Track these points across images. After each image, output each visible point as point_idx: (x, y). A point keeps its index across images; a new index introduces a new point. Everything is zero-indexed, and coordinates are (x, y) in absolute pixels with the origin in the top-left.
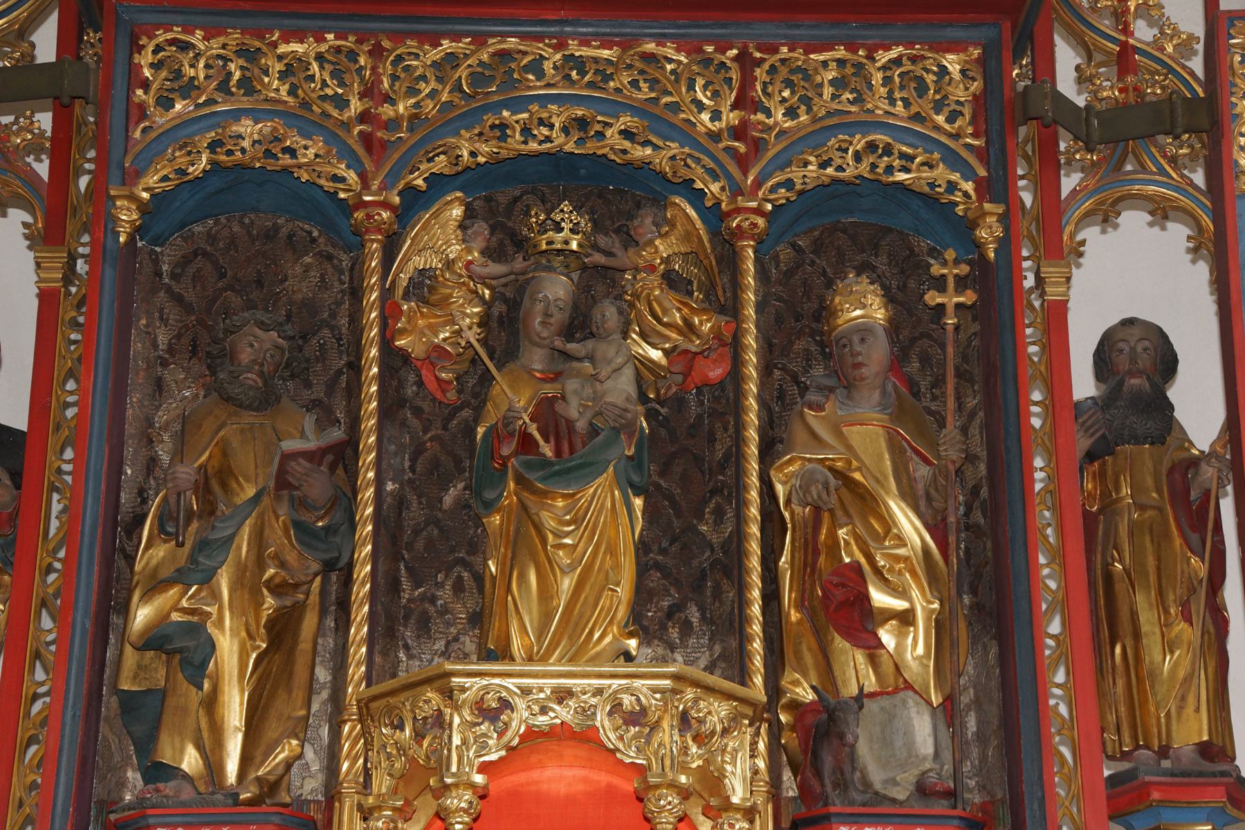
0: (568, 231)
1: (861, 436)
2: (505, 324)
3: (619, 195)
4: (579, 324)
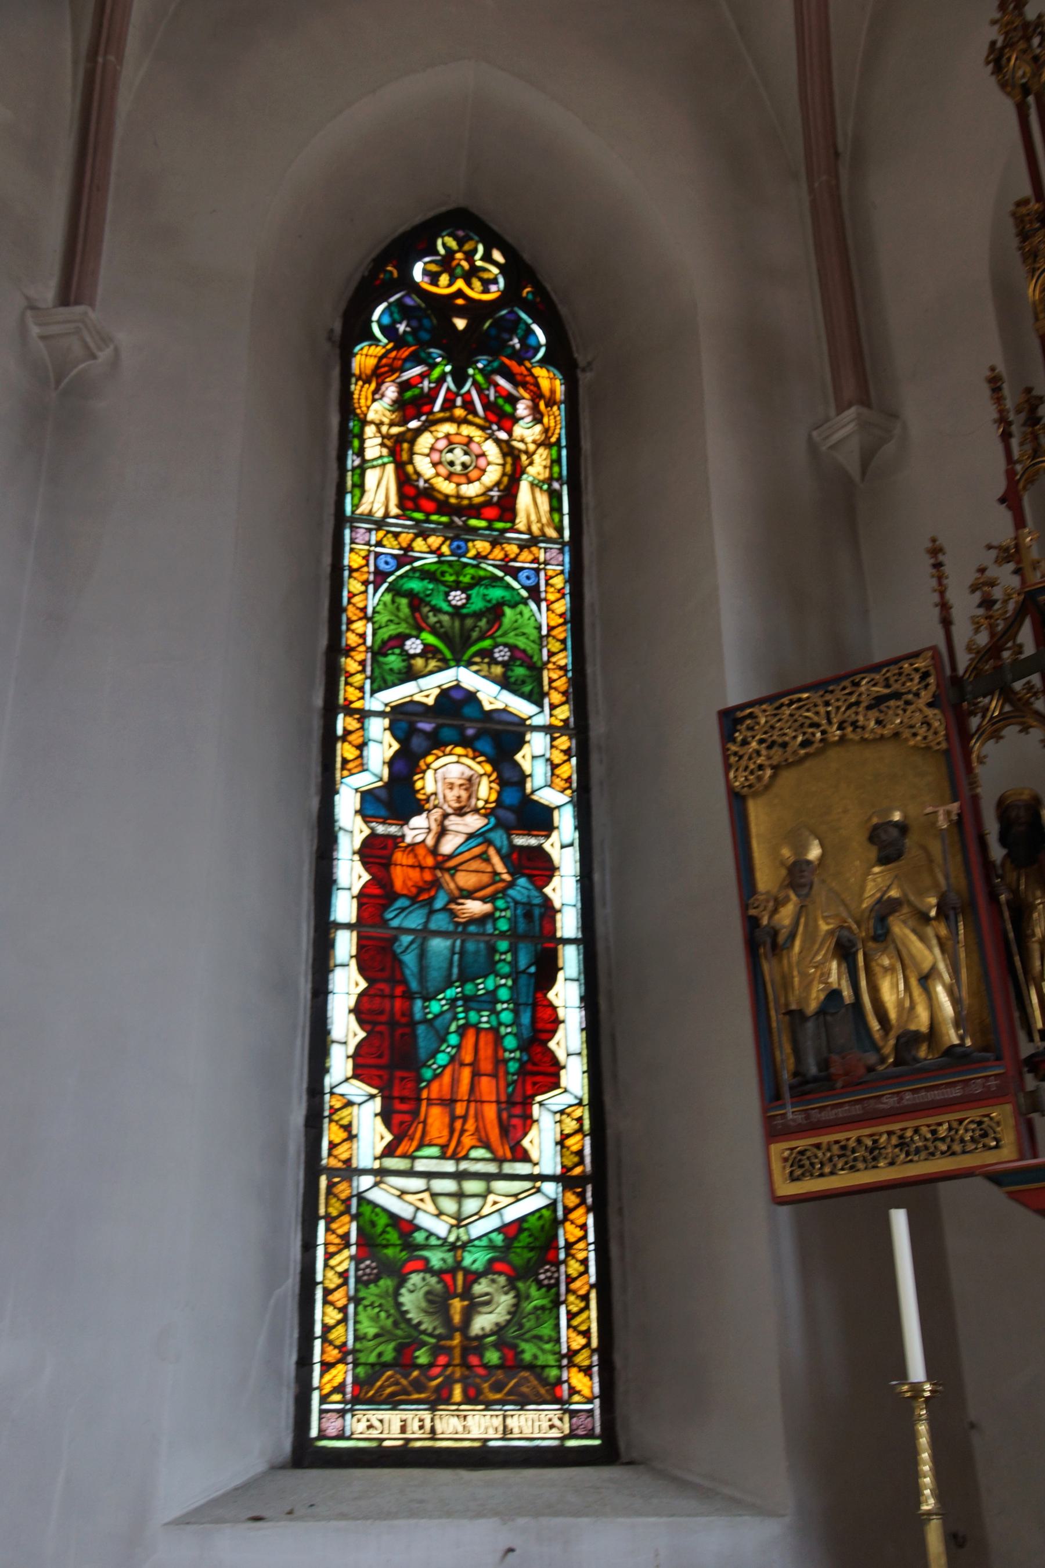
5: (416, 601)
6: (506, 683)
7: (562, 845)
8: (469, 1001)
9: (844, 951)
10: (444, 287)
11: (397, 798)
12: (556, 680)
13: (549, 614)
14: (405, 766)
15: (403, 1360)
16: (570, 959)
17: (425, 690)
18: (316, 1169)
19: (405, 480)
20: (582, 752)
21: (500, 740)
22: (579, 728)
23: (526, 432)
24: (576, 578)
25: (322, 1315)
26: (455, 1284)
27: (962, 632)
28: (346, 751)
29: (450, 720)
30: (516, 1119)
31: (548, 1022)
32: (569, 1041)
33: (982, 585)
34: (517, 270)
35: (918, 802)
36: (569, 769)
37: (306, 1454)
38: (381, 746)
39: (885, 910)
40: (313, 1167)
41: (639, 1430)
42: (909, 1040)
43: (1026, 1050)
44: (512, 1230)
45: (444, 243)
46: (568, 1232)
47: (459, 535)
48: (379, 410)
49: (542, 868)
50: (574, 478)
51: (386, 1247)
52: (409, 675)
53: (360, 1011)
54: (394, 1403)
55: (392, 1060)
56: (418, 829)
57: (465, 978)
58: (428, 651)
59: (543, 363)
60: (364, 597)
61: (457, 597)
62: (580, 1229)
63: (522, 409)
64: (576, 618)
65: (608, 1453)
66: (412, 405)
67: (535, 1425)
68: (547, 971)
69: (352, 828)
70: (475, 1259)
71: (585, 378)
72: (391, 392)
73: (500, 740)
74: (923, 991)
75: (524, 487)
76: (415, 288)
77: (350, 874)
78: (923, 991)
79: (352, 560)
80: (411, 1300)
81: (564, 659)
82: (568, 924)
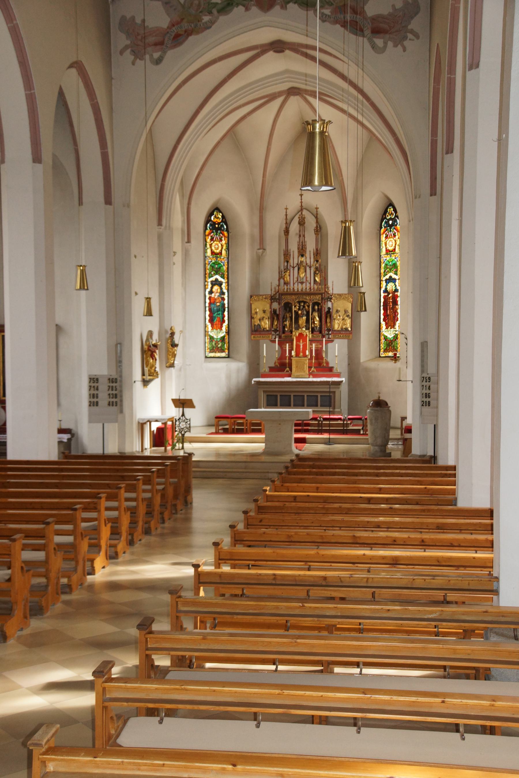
0: (302, 304)
1: (316, 314)
2: (299, 309)
3: (305, 302)
4: (303, 309)
5: (213, 267)
6: (221, 277)
7: (226, 297)
8: (218, 314)
9: (260, 320)
10: (215, 220)
11: (211, 292)
12: (226, 276)
13: (225, 268)
14: (212, 288)
15: (213, 349)
16: (226, 309)
17: (213, 279)
18: (206, 332)
19: (212, 250)
20: (228, 285)
21: (220, 284)
22: (228, 282)
23: (224, 242)
24: (228, 263)
25: (207, 345)
26: (217, 342)
27: (273, 292)
28: (207, 287)
29: (216, 283)
30: (222, 326)
31: (224, 316)
32: (226, 318)
33: (275, 288)
34: (223, 216)
35: (267, 308)
36: (227, 288)
37: (206, 357)
38: (210, 285)
39: (263, 317)
40: (206, 332)
41: (231, 355)
42: (264, 329)
43: (273, 329)
44: (221, 337)
45: (215, 213)
46: (226, 337)
47: (217, 258)
48: (208, 240)
49: (223, 299)
50: (228, 249)
51: (211, 338)
52: (212, 277)
53: (209, 316)
54: (212, 352)
55: (211, 321)
56: (213, 294)
57: (218, 312)
58: (214, 274)
59: (226, 231)
60: (208, 267)
61: (216, 266)
62: (227, 337)
63: (223, 239)
64: (228, 268)
65: (228, 357)
66: (212, 239)
67: (223, 355)
68: (224, 310)
69: (208, 296)
70: (218, 340)
71: (230, 234)
72: (210, 237)
73: (220, 284)
74: (266, 324)
75: (223, 250)
76: (212, 221)
77: (208, 301)
78: (266, 324)
79: (207, 262)
80: (214, 344)
81: (226, 274)
82: (226, 306)
